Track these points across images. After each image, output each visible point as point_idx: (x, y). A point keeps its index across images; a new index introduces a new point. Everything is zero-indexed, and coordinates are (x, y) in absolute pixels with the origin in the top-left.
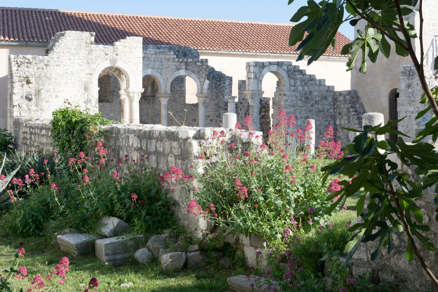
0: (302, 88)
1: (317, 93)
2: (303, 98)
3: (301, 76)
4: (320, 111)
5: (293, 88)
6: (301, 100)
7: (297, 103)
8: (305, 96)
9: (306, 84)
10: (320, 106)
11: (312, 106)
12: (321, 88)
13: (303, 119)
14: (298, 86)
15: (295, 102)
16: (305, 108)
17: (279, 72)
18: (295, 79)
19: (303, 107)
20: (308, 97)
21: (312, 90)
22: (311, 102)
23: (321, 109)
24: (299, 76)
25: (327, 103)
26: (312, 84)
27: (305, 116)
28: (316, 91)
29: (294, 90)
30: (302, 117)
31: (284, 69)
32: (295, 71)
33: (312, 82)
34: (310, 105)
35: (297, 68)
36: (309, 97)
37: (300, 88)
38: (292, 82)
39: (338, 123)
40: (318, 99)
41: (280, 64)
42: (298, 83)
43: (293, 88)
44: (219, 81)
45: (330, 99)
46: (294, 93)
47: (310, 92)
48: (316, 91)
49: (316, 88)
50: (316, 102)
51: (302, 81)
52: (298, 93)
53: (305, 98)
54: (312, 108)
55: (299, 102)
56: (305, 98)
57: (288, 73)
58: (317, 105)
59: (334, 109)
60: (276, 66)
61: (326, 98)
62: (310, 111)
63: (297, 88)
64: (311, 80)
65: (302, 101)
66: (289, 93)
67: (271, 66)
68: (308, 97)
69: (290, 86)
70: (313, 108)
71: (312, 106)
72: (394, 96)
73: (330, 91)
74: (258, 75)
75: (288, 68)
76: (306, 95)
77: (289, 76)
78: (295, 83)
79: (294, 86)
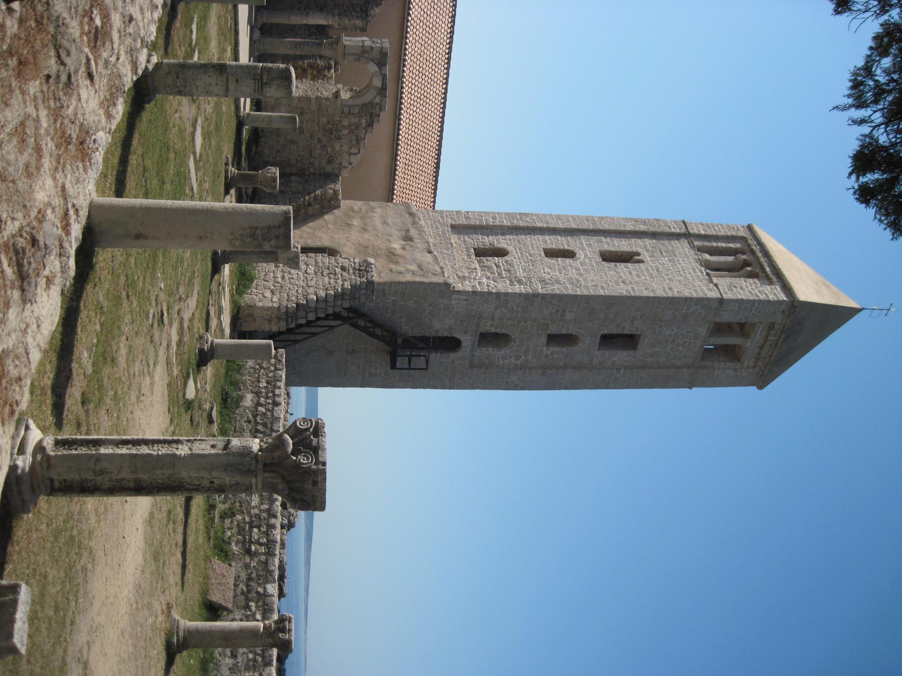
1: (337, 147)
3: (364, 125)
4: (311, 152)
5: (346, 110)
6: (328, 123)
7: (323, 116)
10: (318, 151)
11: (319, 140)
12: (346, 156)
15: (325, 112)
16: (317, 128)
17: (372, 90)
23: (313, 154)
24: (364, 121)
25: (324, 163)
27: (305, 128)
28: (341, 146)
29: (343, 113)
31: (375, 98)
32: (371, 115)
33: (354, 142)
35: (376, 119)
36: (332, 136)
37: (345, 123)
38: (357, 110)
39: (293, 178)
40: (329, 150)
42: (354, 120)
43: (346, 110)
44: (361, 10)
45: (329, 168)
47: (339, 138)
48: (341, 146)
49: (345, 148)
50: (324, 146)
51: (357, 126)
52: (338, 119)
53: (331, 129)
54: (316, 139)
55: (325, 119)
56: (331, 129)
58: (319, 146)
59: (314, 174)
60: (380, 86)
61: (330, 162)
62: (311, 137)
64: (357, 140)
66: (339, 105)
67: (380, 78)
72: (331, 252)
73: (340, 170)
74: (367, 55)
75: (377, 104)
77: (364, 105)
79: (349, 113)
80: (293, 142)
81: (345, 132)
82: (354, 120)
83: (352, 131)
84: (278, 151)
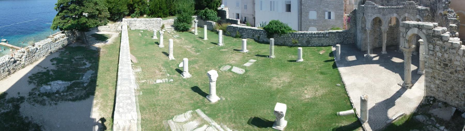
0: (441, 54)
1: (458, 63)
2: (442, 64)
5: (431, 52)
6: (439, 65)
7: (435, 67)
8: (444, 63)
9: (446, 51)
10: (460, 76)
11: (451, 73)
13: (441, 81)
14: (437, 51)
18: (435, 45)
19: (441, 71)
20: (447, 64)
21: (453, 59)
22: (451, 70)
24: (438, 42)
26: (453, 53)
27: (443, 79)
29: (433, 55)
30: (439, 79)
34: (449, 72)
35: (436, 34)
36: (449, 64)
37: (439, 54)
38: (431, 46)
40: (458, 69)
41: (420, 27)
42: (437, 48)
46: (433, 58)
47: (451, 60)
49: (458, 58)
51: (442, 47)
52: (437, 59)
53: (444, 64)
55: (437, 66)
56: (444, 64)
57: (427, 38)
58: (456, 75)
63: (436, 53)
64: (453, 49)
65: (440, 67)
66: (428, 56)
68: (447, 64)
69: (429, 50)
70: (452, 76)
71: (451, 73)
76: (445, 61)
78: (434, 48)
79: (433, 51)
80: (452, 88)
81: (446, 56)
82: (437, 48)
83: (446, 51)
84: (457, 97)
